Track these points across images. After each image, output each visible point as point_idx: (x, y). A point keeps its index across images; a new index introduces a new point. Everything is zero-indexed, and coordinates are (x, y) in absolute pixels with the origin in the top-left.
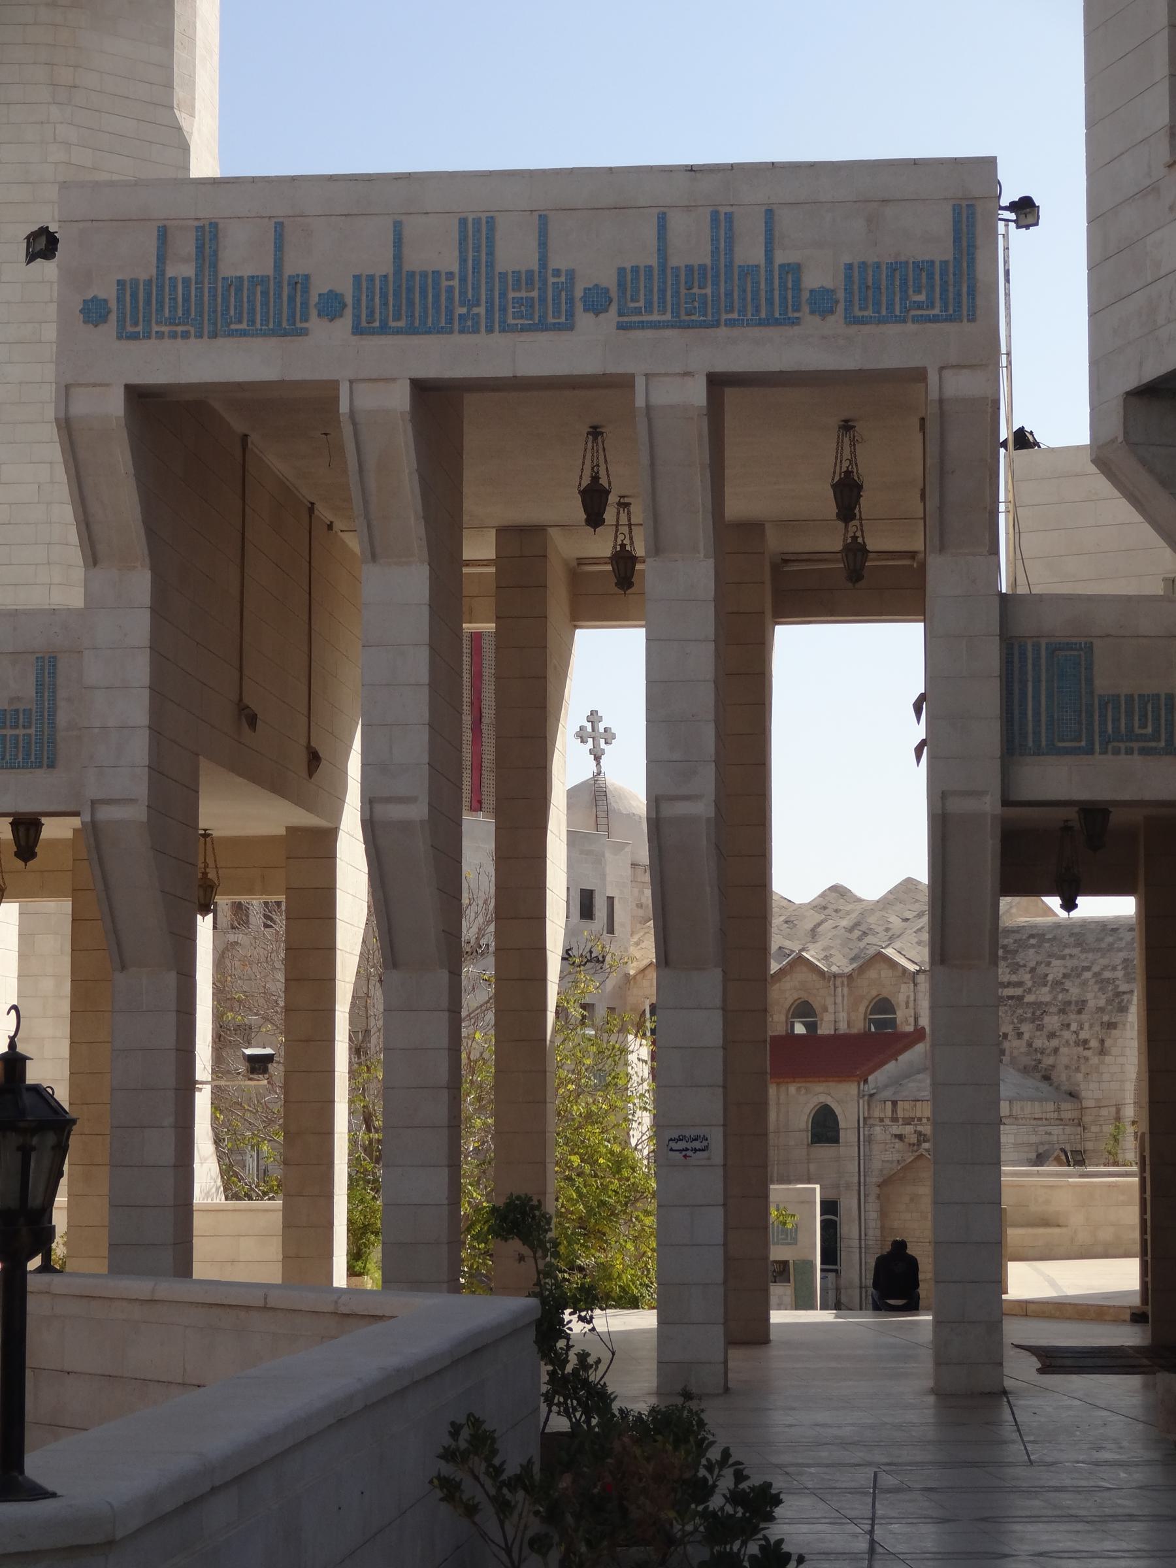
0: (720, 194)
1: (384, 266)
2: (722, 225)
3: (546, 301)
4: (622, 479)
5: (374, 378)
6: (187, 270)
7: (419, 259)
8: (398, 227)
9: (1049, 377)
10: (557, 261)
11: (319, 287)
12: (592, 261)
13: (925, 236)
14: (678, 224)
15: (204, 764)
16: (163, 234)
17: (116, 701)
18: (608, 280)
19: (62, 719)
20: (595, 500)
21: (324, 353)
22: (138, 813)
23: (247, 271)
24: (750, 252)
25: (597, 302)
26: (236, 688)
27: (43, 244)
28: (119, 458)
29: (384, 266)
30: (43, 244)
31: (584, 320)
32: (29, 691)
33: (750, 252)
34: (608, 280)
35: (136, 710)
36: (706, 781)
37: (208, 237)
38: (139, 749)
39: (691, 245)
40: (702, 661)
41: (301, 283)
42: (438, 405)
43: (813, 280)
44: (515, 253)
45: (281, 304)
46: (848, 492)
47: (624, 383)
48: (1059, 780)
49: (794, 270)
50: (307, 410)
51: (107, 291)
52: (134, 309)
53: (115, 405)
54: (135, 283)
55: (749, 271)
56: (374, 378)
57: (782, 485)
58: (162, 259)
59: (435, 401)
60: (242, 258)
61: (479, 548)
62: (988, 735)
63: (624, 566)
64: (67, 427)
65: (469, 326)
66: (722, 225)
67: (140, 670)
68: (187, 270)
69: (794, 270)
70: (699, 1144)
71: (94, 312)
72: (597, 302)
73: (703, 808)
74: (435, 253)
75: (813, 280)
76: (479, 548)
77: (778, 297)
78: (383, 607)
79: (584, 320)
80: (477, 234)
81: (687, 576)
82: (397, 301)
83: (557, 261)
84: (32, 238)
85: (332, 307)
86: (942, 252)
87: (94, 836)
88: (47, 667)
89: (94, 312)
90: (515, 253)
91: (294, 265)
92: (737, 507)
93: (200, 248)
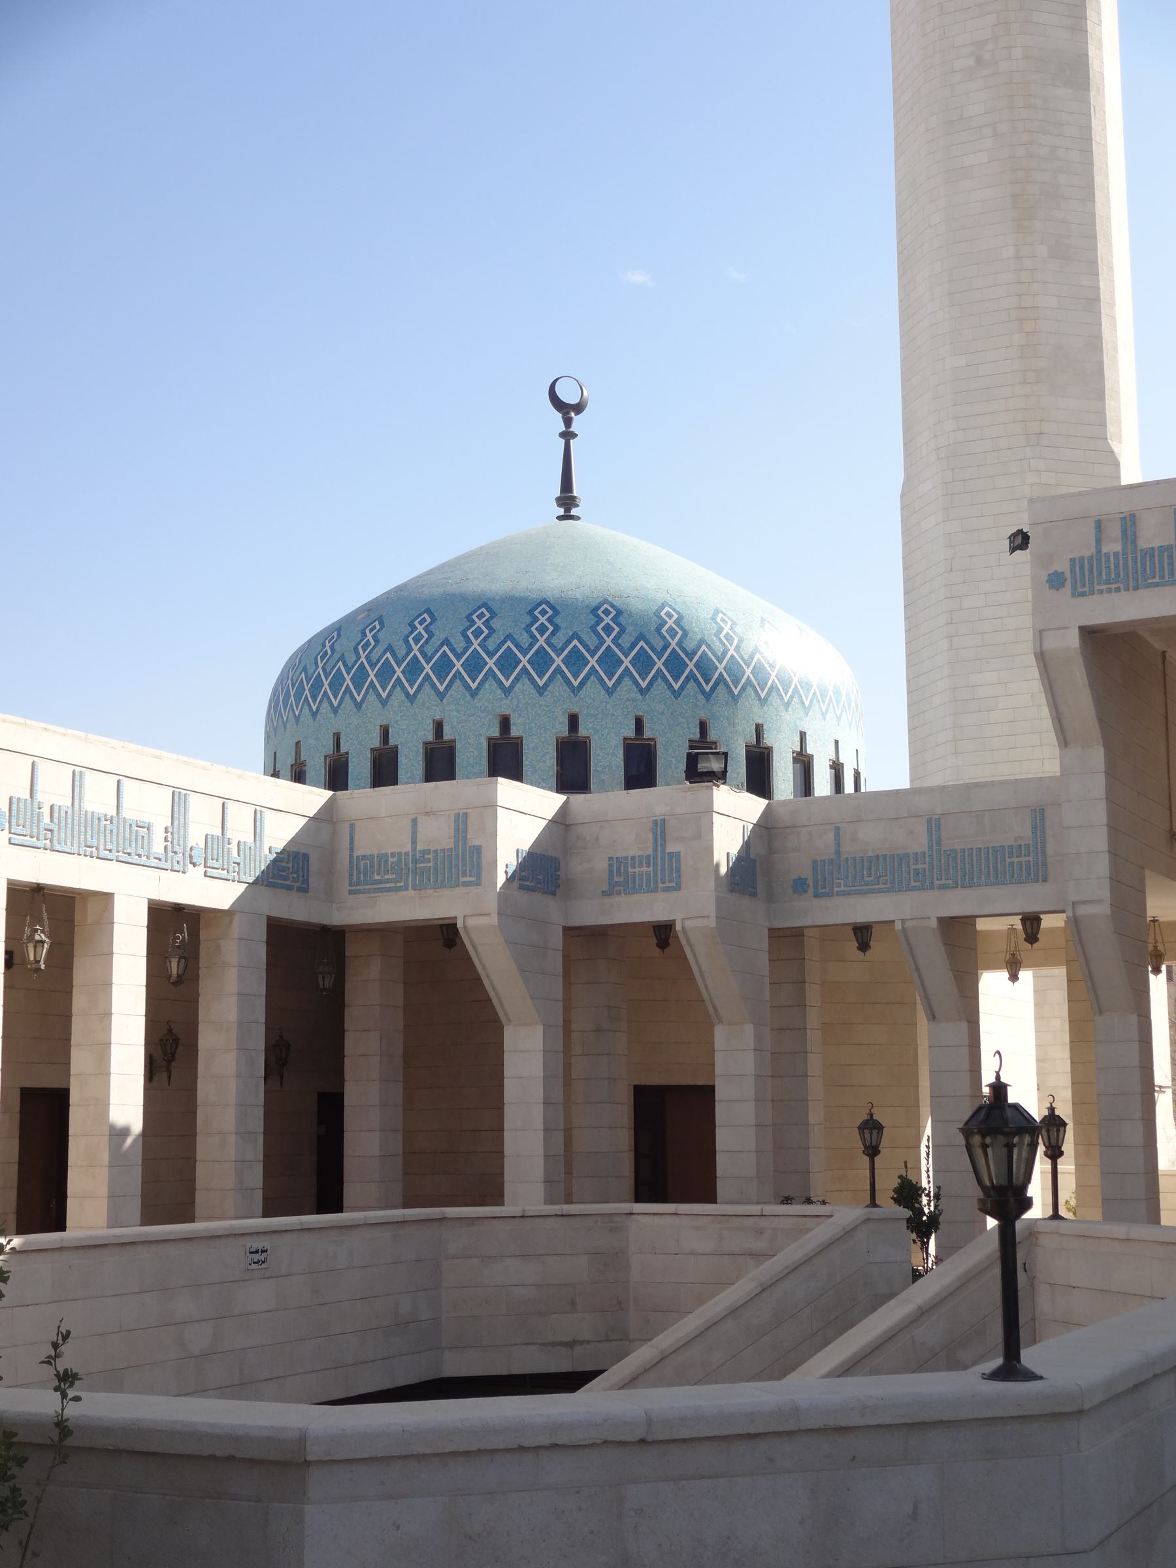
6: (1117, 547)
15: (1148, 873)
16: (1099, 525)
19: (1050, 850)
22: (1104, 909)
23: (1157, 543)
27: (1020, 540)
28: (1077, 675)
30: (1020, 540)
32: (1027, 831)
35: (1100, 841)
37: (1129, 524)
38: (1102, 866)
51: (1065, 567)
52: (1082, 576)
53: (1073, 640)
54: (1082, 559)
58: (1099, 542)
64: (1042, 658)
67: (1100, 814)
68: (1117, 547)
71: (1056, 581)
84: (1013, 537)
87: (1075, 923)
88: (1039, 816)
89: (1056, 581)
93: (1124, 532)
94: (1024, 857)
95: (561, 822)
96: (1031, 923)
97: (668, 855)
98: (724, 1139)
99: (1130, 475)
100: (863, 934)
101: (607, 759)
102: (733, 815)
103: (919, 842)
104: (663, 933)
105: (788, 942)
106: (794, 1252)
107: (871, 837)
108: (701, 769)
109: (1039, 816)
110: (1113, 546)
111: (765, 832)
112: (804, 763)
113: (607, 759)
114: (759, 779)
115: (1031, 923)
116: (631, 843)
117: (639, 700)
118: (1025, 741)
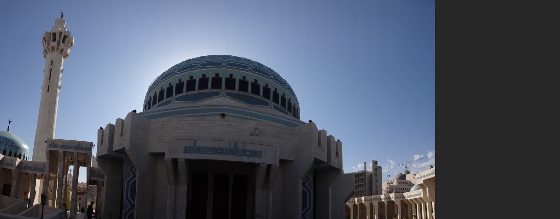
2: (79, 144)
3: (70, 147)
4: (73, 157)
5: (61, 151)
9: (94, 153)
12: (73, 145)
13: (89, 146)
17: (47, 168)
20: (72, 159)
21: (58, 149)
26: (53, 169)
27: (46, 142)
30: (46, 142)
37: (54, 142)
42: (65, 152)
45: (57, 146)
46: (85, 159)
48: (93, 178)
50: (58, 152)
57: (81, 158)
59: (65, 152)
60: (56, 144)
61: (66, 160)
63: (73, 162)
66: (79, 144)
74: (65, 144)
76: (66, 160)
77: (82, 148)
78: (60, 164)
81: (76, 164)
82: (63, 147)
87: (46, 176)
88: (44, 166)
92: (79, 159)
94: (42, 170)
95: (3, 158)
96: (42, 175)
97: (12, 163)
98: (12, 191)
99: (54, 138)
100: (27, 174)
101: (7, 153)
102: (18, 161)
103: (33, 166)
104: (10, 170)
105: (21, 173)
106: (18, 203)
107: (30, 165)
108: (16, 156)
109: (44, 166)
111: (21, 162)
112: (24, 156)
113: (7, 153)
114: (20, 158)
115: (42, 175)
116: (9, 161)
117: (12, 149)
118: (43, 159)
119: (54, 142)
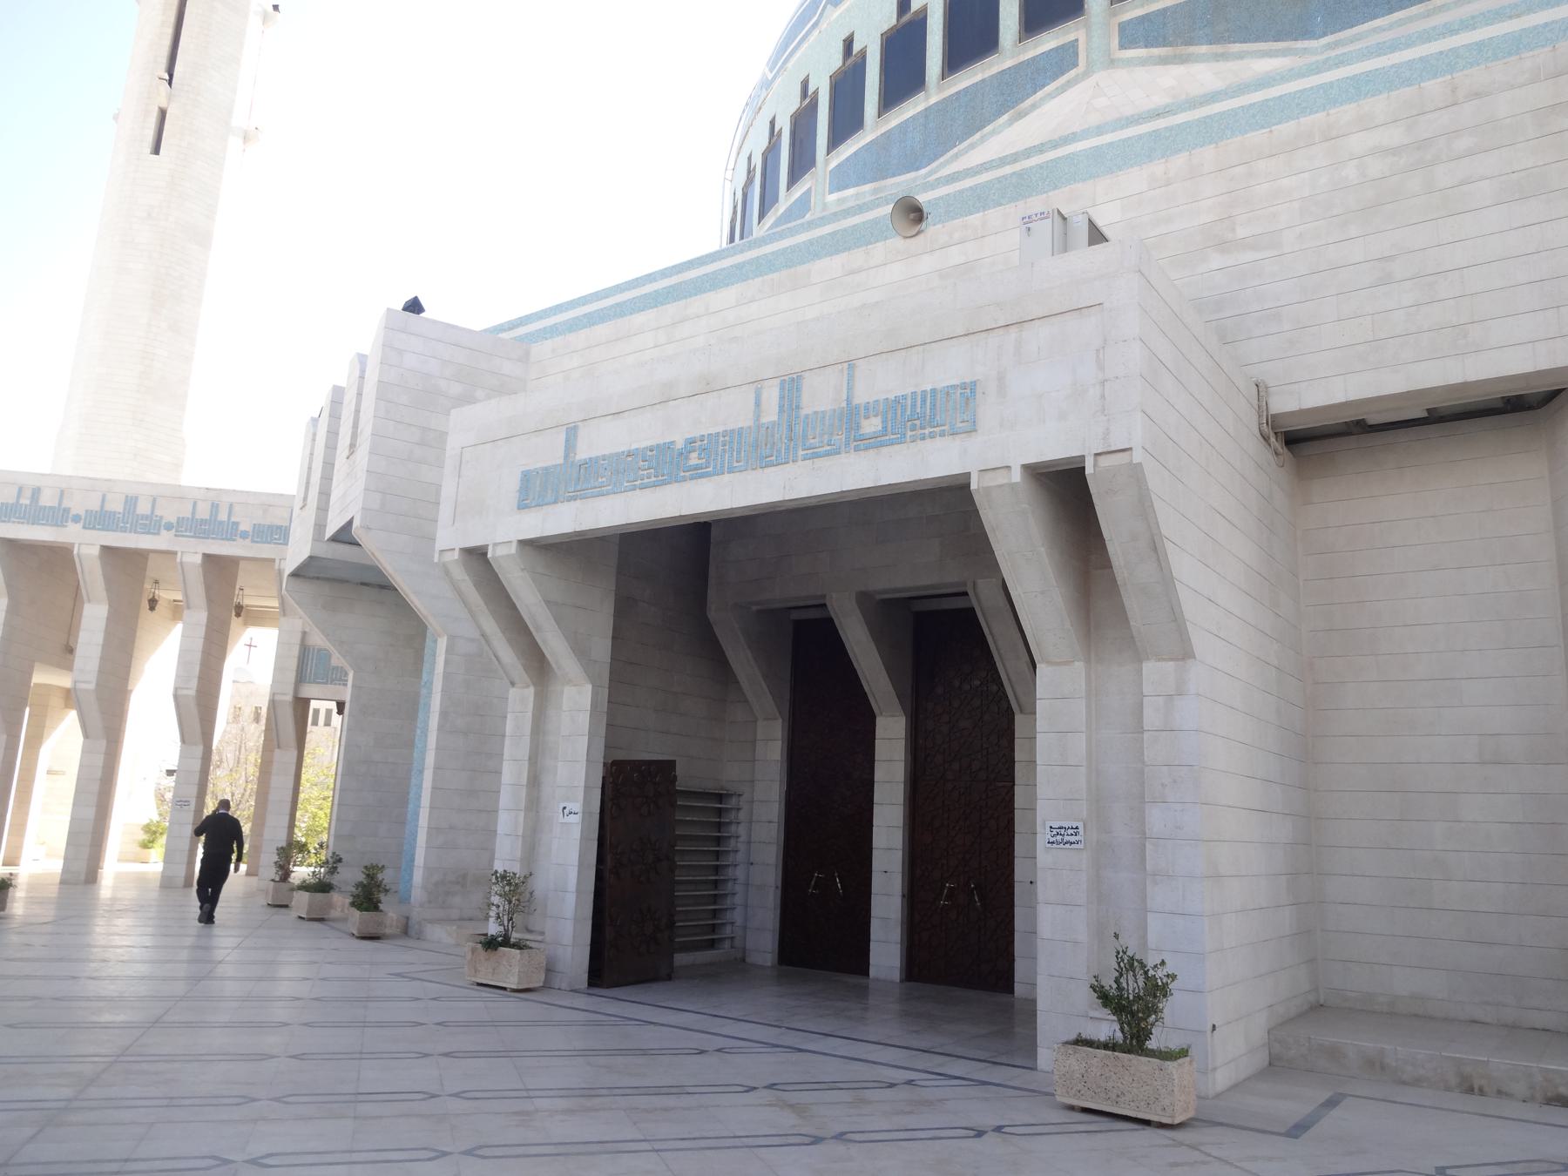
0: (215, 500)
1: (97, 508)
2: (215, 507)
7: (110, 507)
8: (104, 496)
10: (158, 512)
11: (73, 512)
12: (169, 514)
14: (200, 506)
16: (20, 489)
18: (174, 520)
21: (69, 534)
24: (223, 516)
25: (169, 527)
29: (97, 508)
31: (164, 532)
33: (223, 516)
34: (174, 520)
36: (194, 683)
37: (36, 492)
39: (203, 512)
40: (199, 644)
41: (67, 510)
43: (242, 528)
44: (143, 508)
47: (175, 553)
49: (236, 524)
55: (221, 523)
56: (87, 545)
58: (18, 497)
60: (47, 499)
62: (291, 676)
65: (124, 530)
66: (215, 507)
69: (236, 524)
70: (186, 804)
72: (169, 527)
73: (192, 693)
75: (242, 528)
77: (231, 531)
79: (164, 532)
80: (131, 501)
82: (99, 519)
83: (158, 512)
85: (76, 519)
86: (285, 524)
90: (143, 508)
91: (66, 504)
110: (25, 501)
119: (36, 492)
